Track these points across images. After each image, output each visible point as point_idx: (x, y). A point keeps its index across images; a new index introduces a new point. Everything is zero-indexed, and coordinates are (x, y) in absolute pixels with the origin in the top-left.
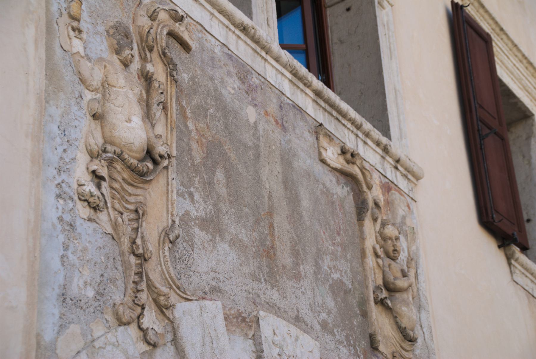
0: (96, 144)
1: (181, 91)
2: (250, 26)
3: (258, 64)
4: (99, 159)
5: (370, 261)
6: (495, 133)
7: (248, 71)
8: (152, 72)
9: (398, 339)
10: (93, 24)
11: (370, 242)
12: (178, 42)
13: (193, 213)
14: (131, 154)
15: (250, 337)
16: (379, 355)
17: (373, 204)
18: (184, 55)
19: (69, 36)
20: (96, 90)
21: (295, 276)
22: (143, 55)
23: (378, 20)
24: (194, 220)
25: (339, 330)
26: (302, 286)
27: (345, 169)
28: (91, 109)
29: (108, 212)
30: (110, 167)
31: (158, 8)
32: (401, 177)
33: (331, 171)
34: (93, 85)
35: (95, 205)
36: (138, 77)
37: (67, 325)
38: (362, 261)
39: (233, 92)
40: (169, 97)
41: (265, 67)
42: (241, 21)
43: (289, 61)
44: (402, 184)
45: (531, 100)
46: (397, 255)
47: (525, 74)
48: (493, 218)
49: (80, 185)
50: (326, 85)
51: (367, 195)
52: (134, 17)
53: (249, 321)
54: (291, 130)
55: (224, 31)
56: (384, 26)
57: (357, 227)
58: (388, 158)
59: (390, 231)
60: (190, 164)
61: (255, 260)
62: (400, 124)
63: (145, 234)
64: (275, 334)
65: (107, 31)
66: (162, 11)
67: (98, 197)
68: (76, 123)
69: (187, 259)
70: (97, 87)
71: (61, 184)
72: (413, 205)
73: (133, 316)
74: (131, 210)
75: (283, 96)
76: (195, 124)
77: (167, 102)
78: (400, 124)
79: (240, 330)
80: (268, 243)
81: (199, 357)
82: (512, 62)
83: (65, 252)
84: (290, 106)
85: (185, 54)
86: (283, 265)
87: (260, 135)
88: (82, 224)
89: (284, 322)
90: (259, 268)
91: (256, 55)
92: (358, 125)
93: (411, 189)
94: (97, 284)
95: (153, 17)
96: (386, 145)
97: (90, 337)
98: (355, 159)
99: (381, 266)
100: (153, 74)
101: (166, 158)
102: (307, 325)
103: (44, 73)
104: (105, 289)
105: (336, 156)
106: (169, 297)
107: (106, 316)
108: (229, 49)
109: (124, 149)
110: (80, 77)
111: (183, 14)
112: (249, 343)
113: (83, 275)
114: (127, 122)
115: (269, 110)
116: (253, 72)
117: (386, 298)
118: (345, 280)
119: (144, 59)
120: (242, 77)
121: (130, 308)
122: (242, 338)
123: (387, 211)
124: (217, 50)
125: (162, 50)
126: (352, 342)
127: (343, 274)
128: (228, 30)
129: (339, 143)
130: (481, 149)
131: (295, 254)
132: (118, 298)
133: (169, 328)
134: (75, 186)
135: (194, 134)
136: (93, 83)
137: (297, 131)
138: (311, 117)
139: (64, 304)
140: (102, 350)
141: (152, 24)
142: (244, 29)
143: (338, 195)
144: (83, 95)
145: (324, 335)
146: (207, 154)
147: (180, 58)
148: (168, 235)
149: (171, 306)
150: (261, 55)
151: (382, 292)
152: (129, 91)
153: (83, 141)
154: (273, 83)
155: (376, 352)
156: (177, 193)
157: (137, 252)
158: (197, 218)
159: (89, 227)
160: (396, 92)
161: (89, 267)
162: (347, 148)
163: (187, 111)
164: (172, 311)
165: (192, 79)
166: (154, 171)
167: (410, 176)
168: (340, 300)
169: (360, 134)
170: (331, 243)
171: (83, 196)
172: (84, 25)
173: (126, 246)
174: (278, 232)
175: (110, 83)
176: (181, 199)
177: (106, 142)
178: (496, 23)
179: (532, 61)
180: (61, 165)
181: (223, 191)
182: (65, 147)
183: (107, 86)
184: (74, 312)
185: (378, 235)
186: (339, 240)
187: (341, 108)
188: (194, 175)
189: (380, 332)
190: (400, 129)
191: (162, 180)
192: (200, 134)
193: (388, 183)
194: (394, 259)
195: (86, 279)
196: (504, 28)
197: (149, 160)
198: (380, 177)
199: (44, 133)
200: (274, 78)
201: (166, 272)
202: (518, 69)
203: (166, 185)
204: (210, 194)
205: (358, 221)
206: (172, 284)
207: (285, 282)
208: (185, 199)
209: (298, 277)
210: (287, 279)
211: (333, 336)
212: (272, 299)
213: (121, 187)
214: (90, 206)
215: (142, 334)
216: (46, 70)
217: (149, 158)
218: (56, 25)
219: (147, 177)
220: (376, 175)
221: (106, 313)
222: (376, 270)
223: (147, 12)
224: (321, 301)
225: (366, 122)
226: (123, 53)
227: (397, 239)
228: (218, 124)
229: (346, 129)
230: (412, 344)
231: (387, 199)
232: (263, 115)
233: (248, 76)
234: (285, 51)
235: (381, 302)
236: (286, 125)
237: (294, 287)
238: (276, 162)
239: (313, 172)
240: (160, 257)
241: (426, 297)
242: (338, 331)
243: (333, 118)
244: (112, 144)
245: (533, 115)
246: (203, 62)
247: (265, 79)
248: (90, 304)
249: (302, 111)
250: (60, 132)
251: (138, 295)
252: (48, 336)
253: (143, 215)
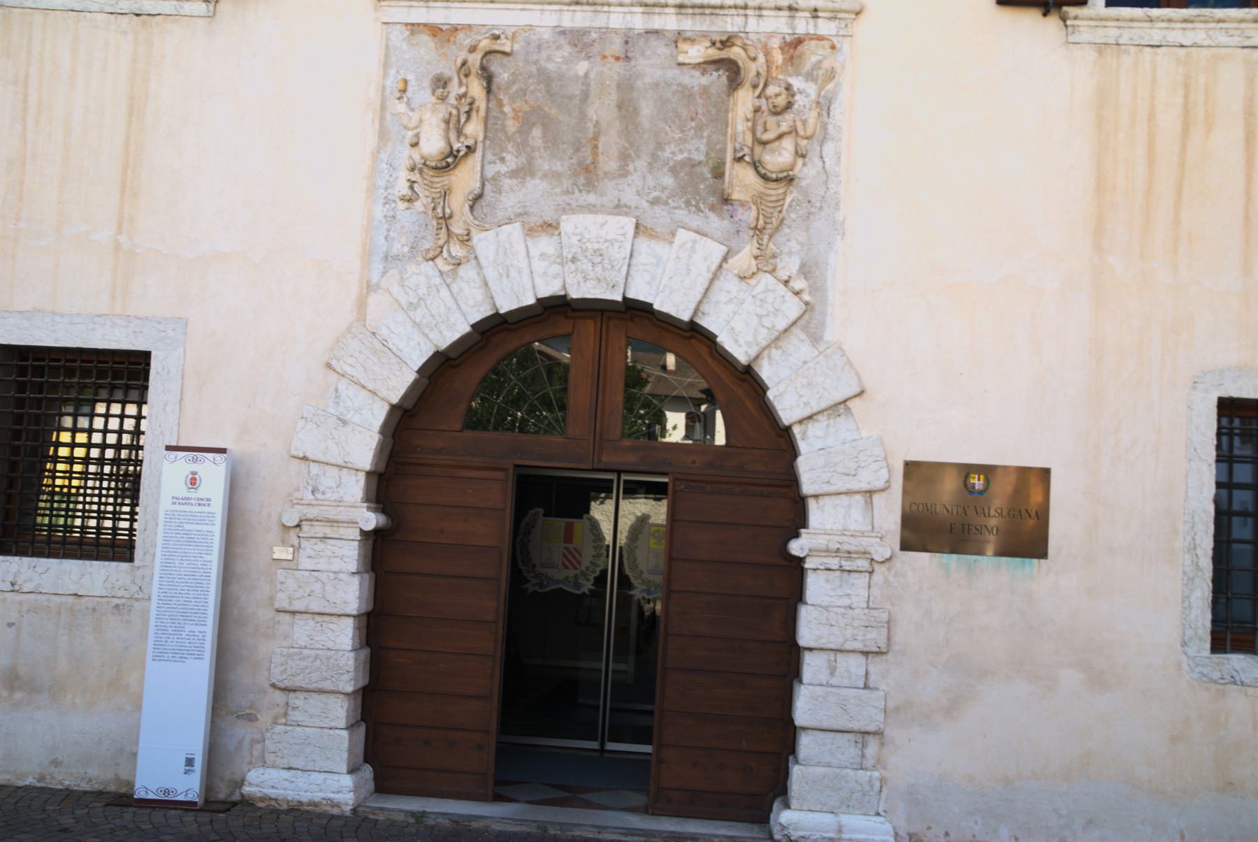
167: (840, 15)
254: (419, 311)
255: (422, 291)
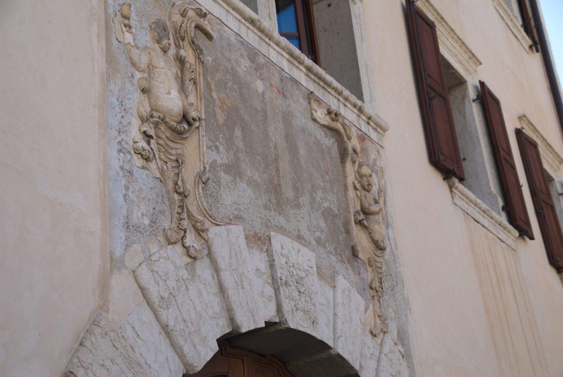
0: (145, 111)
1: (206, 70)
2: (257, 19)
3: (263, 48)
4: (148, 122)
5: (351, 193)
6: (440, 95)
7: (256, 53)
8: (184, 56)
9: (372, 249)
10: (140, 21)
11: (351, 179)
12: (203, 33)
13: (219, 161)
14: (172, 118)
15: (264, 251)
16: (360, 261)
17: (352, 150)
18: (208, 42)
19: (122, 31)
20: (143, 71)
21: (296, 206)
22: (177, 44)
23: (352, 12)
24: (220, 166)
25: (330, 244)
26: (301, 213)
27: (331, 125)
28: (141, 85)
29: (156, 162)
30: (157, 129)
31: (187, 7)
32: (372, 130)
33: (320, 127)
34: (141, 67)
35: (146, 157)
36: (174, 60)
37: (131, 244)
38: (345, 193)
39: (245, 69)
40: (198, 74)
41: (269, 50)
42: (250, 16)
43: (286, 45)
44: (373, 135)
45: (465, 71)
46: (370, 188)
47: (460, 52)
48: (439, 158)
49: (135, 142)
50: (314, 62)
51: (347, 144)
52: (169, 15)
53: (263, 239)
54: (289, 97)
55: (237, 23)
56: (357, 17)
57: (341, 168)
58: (362, 116)
59: (365, 170)
60: (215, 125)
61: (266, 195)
62: (370, 90)
63: (184, 178)
64: (282, 248)
65: (150, 27)
66: (191, 10)
67: (149, 151)
68: (130, 96)
69: (216, 195)
70: (144, 69)
71: (121, 142)
72: (381, 151)
73: (178, 237)
74: (173, 160)
75: (283, 72)
76: (218, 95)
77: (196, 79)
78: (370, 90)
79: (257, 246)
80: (275, 182)
81: (228, 266)
82: (450, 42)
83: (127, 192)
84: (288, 79)
85: (208, 42)
86: (287, 198)
87: (266, 101)
88: (138, 171)
89: (289, 239)
90: (270, 200)
91: (262, 41)
92: (339, 92)
93: (379, 139)
94: (151, 215)
95: (184, 14)
96: (361, 107)
97: (148, 253)
98: (338, 118)
99: (359, 196)
100: (185, 57)
101: (197, 121)
102: (306, 241)
103: (105, 60)
104: (157, 219)
105: (324, 115)
106: (204, 224)
107: (159, 238)
108: (241, 37)
109: (166, 115)
110: (132, 62)
111: (206, 11)
112: (264, 255)
113: (140, 208)
114: (167, 94)
115: (272, 82)
116: (260, 54)
117: (363, 219)
118: (332, 207)
119: (178, 47)
120: (252, 58)
121: (176, 232)
122: (259, 252)
123: (363, 155)
124: (232, 38)
125: (191, 39)
126: (339, 252)
127: (331, 203)
128: (240, 23)
129: (326, 106)
130: (430, 107)
131: (296, 189)
132: (166, 224)
133: (205, 246)
134: (132, 143)
135: (218, 103)
136: (141, 66)
137: (294, 98)
138: (304, 87)
139: (128, 229)
140: (157, 262)
141: (183, 20)
142: (252, 22)
143: (326, 145)
144: (134, 75)
145: (318, 248)
146: (228, 117)
147: (205, 45)
148: (201, 177)
149: (205, 230)
150: (265, 41)
151: (360, 215)
152: (168, 71)
153: (135, 109)
154: (275, 62)
155: (357, 259)
156: (207, 147)
157: (179, 191)
158: (222, 165)
159: (143, 173)
160: (366, 67)
161: (144, 202)
162: (332, 109)
163: (212, 85)
164: (207, 233)
165: (214, 60)
166: (189, 130)
167: (379, 130)
168: (329, 222)
169: (341, 99)
170: (322, 181)
171: (137, 150)
172: (133, 22)
173: (170, 187)
174: (283, 173)
175: (153, 65)
176: (210, 151)
177: (152, 110)
178: (438, 13)
179: (464, 41)
180: (120, 127)
181: (241, 144)
182: (123, 114)
183: (152, 68)
184: (135, 235)
185: (356, 173)
186: (328, 178)
187: (326, 80)
188: (218, 132)
189: (359, 244)
190: (371, 94)
191: (195, 137)
192: (222, 102)
193: (363, 135)
194: (368, 191)
195: (143, 211)
196: (444, 17)
197: (184, 122)
198: (357, 131)
199: (107, 104)
200: (276, 58)
201: (201, 205)
202: (455, 48)
203: (198, 141)
204: (231, 147)
205: (341, 164)
206: (205, 214)
207: (289, 210)
208: (212, 151)
209: (298, 206)
210: (291, 208)
211: (325, 248)
212: (279, 223)
213: (165, 143)
214: (143, 158)
215: (185, 250)
216: (106, 57)
217: (185, 121)
218: (112, 23)
219: (184, 135)
220: (354, 129)
221: (159, 236)
222: (355, 199)
223: (179, 11)
224: (315, 223)
225: (346, 89)
226: (162, 42)
227: (370, 176)
228: (236, 94)
229: (331, 95)
230: (382, 252)
231: (363, 147)
232: (269, 86)
233: (256, 58)
234: (283, 37)
235: (360, 223)
236: (286, 93)
237: (296, 214)
238: (279, 122)
239: (307, 128)
240: (196, 194)
241: (392, 218)
242: (328, 244)
243: (321, 87)
244: (157, 111)
245: (466, 81)
246: (222, 47)
247: (269, 59)
248: (146, 229)
249: (298, 83)
250: (118, 103)
251: (181, 222)
252: (118, 252)
253: (182, 163)
254: (171, 310)
255: (172, 283)
